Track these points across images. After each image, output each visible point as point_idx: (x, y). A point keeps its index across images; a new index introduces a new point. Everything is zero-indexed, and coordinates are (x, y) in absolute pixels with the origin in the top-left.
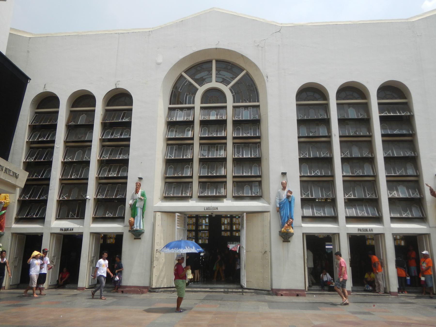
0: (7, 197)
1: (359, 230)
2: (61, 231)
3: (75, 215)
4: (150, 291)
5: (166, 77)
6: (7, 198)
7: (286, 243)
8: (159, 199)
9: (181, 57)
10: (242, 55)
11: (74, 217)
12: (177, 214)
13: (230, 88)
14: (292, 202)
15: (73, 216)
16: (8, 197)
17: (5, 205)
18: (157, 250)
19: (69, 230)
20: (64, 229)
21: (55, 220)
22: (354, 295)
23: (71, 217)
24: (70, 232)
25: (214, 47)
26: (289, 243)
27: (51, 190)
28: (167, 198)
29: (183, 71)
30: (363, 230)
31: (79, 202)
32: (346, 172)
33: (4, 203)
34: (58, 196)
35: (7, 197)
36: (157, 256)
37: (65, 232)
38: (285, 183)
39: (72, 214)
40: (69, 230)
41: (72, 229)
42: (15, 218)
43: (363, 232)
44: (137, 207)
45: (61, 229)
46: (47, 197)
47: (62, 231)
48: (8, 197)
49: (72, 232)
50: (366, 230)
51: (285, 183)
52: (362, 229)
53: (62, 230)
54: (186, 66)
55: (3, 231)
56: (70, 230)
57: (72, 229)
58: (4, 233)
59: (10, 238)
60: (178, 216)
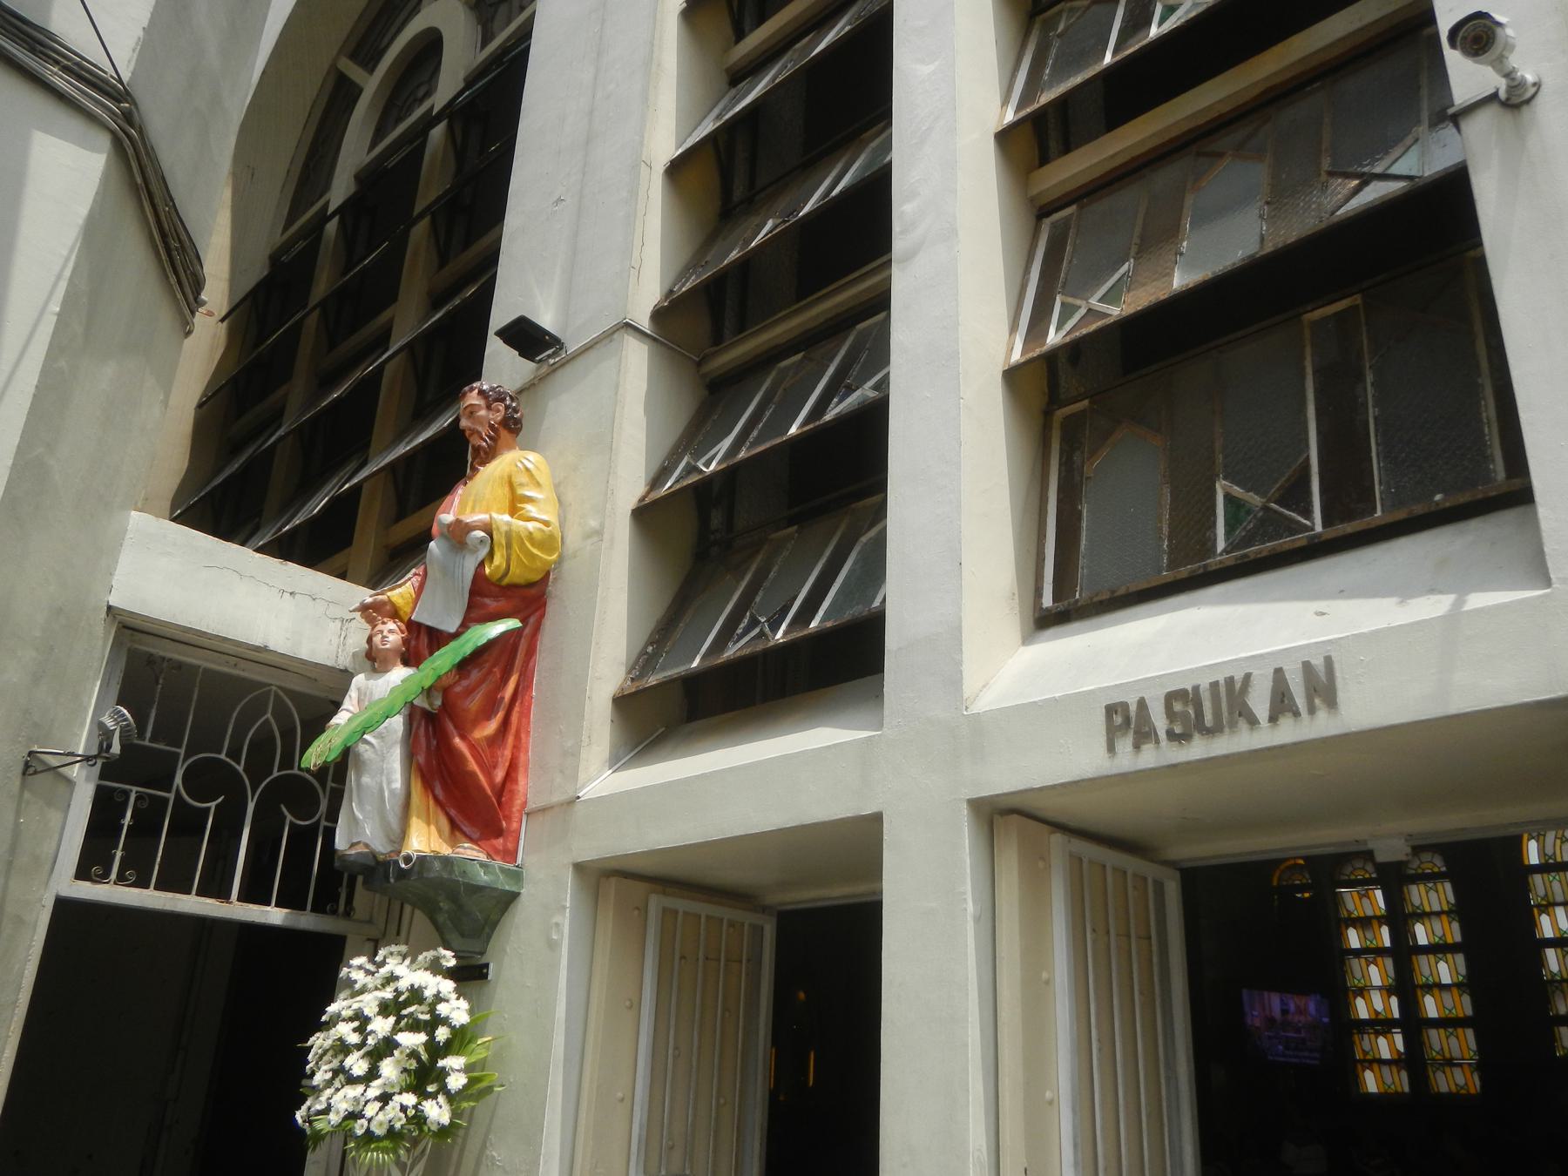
0: (521, 491)
2: (1125, 745)
3: (1296, 495)
6: (530, 500)
11: (1296, 528)
15: (1271, 525)
16: (538, 485)
17: (499, 559)
19: (1260, 703)
20: (1171, 698)
21: (1027, 640)
23: (1248, 541)
24: (1288, 732)
27: (910, 255)
31: (1318, 314)
33: (480, 534)
34: (1014, 328)
35: (521, 485)
37: (1198, 749)
39: (1255, 500)
40: (1260, 703)
41: (1307, 666)
42: (624, 703)
45: (1111, 710)
46: (883, 385)
47: (1137, 747)
48: (538, 485)
49: (1321, 725)
53: (1144, 734)
55: (510, 855)
56: (1282, 704)
57: (1307, 666)
58: (517, 876)
59: (565, 924)
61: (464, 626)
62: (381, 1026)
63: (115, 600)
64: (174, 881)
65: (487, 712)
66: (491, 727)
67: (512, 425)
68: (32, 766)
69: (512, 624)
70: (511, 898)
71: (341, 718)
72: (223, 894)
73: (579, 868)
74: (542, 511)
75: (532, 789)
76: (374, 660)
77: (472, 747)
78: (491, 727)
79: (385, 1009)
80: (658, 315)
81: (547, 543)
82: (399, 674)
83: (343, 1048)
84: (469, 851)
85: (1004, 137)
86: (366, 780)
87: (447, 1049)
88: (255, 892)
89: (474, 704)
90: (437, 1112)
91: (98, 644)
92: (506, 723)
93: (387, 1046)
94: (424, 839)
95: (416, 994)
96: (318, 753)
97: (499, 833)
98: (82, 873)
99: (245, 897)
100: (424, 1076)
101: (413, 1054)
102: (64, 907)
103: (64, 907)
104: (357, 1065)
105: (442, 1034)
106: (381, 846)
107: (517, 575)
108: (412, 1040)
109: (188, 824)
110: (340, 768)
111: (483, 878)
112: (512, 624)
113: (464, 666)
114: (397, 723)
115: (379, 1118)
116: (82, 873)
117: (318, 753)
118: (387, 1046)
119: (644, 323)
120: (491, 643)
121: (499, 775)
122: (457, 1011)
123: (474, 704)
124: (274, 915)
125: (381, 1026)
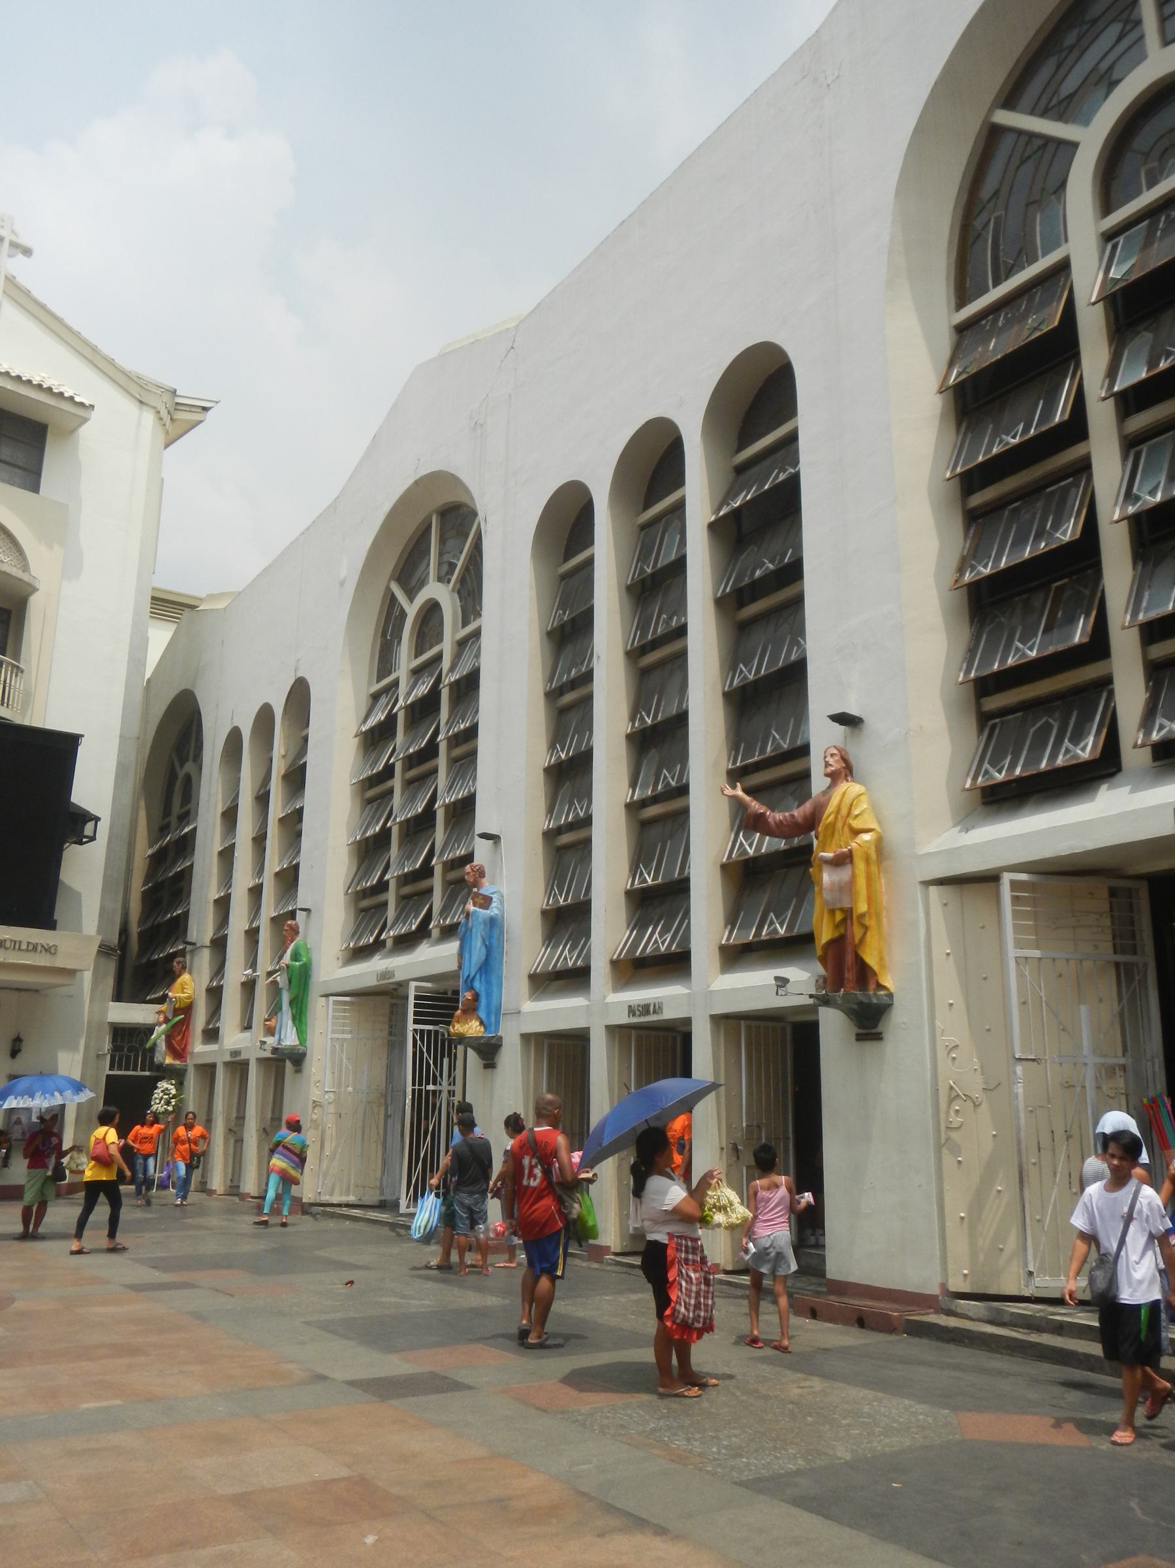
1: (631, 1010)
4: (305, 1213)
5: (354, 614)
7: (489, 1071)
8: (338, 959)
9: (369, 542)
10: (452, 475)
12: (332, 999)
13: (457, 588)
14: (474, 930)
16: (186, 984)
17: (178, 1004)
18: (314, 1102)
22: (610, 1264)
25: (411, 481)
26: (495, 1070)
28: (359, 953)
29: (392, 578)
30: (640, 1009)
32: (644, 787)
36: (315, 1117)
38: (470, 871)
43: (640, 1016)
44: (281, 989)
50: (645, 1009)
51: (470, 871)
52: (639, 1006)
54: (390, 564)
58: (186, 1066)
60: (335, 1002)
61: (173, 1018)
62: (161, 1095)
63: (109, 1021)
64: (127, 1069)
65: (179, 1035)
66: (179, 1038)
67: (184, 968)
68: (98, 1056)
69: (183, 1016)
70: (186, 1070)
71: (152, 1037)
72: (136, 1070)
73: (195, 1065)
74: (190, 991)
75: (189, 1048)
76: (160, 1024)
77: (177, 1042)
78: (179, 1038)
79: (162, 1091)
80: (213, 941)
81: (189, 998)
82: (164, 1026)
83: (156, 1099)
84: (177, 1062)
85: (246, 932)
86: (159, 1049)
87: (172, 1098)
88: (143, 1070)
89: (176, 1034)
90: (170, 1108)
91: (107, 1029)
92: (184, 1035)
93: (161, 1099)
94: (169, 1060)
95: (167, 1089)
96: (148, 1045)
97: (183, 1057)
98: (110, 1070)
99: (141, 1070)
100: (168, 1103)
101: (166, 1099)
102: (108, 1076)
103: (108, 1076)
104: (158, 1101)
105: (171, 1096)
106: (162, 1061)
107: (182, 1006)
108: (165, 1097)
109: (128, 1058)
110: (155, 1044)
111: (179, 1067)
112: (183, 1016)
113: (173, 1026)
114: (163, 1037)
115: (162, 1110)
116: (110, 1070)
117: (148, 1045)
118: (161, 1099)
119: (208, 944)
120: (178, 1022)
121: (183, 1046)
122: (174, 1092)
123: (176, 1034)
124: (147, 1073)
125: (161, 1095)
